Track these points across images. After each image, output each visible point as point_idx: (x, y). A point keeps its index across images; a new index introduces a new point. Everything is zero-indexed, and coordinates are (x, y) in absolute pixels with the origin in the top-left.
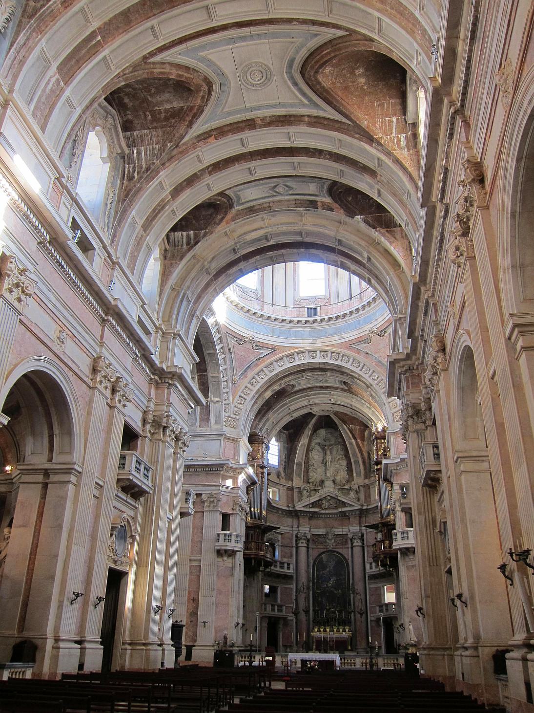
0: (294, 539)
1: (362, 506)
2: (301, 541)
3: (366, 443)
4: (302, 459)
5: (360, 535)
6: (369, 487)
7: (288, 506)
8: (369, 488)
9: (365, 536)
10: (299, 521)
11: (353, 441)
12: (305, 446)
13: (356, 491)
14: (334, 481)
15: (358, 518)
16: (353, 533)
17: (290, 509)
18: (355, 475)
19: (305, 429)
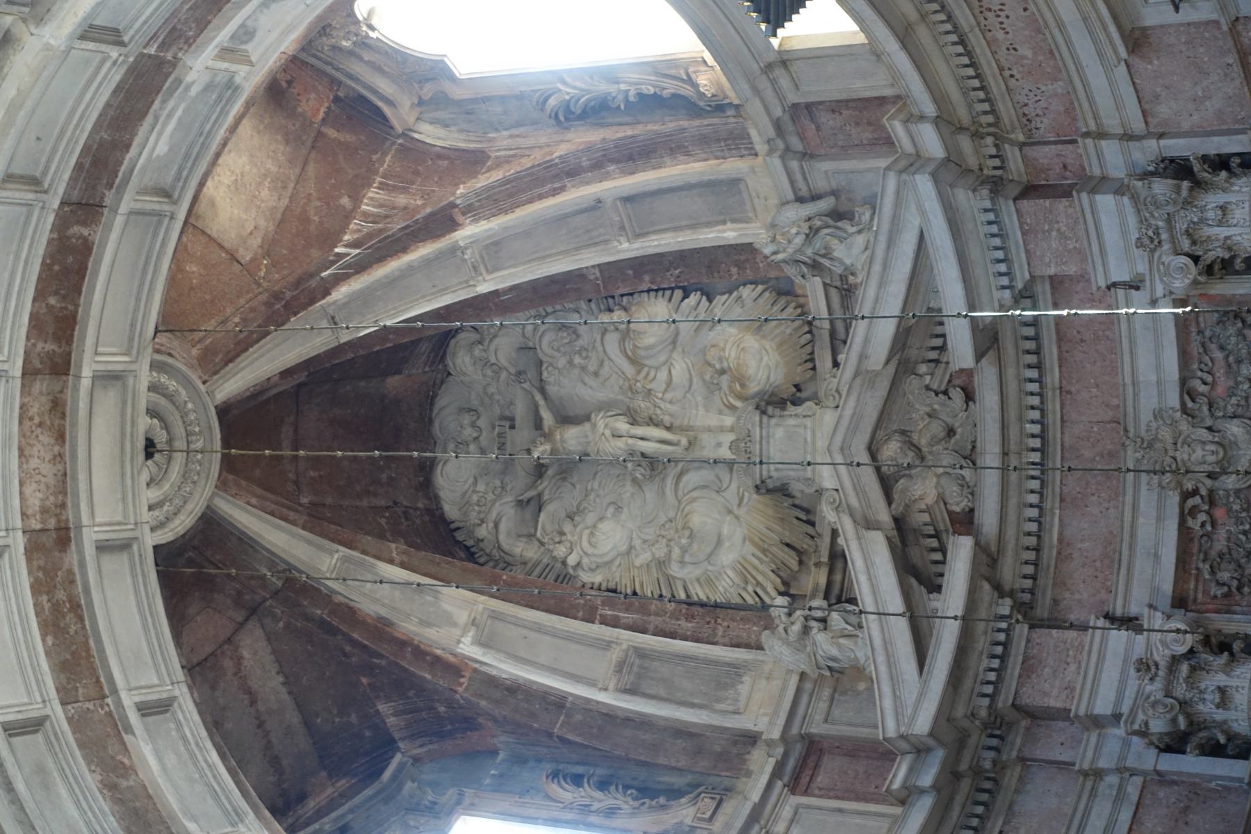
0: (1191, 764)
1: (915, 162)
2: (1207, 709)
3: (501, 142)
4: (608, 645)
5: (1161, 187)
6: (795, 106)
7: (905, 798)
8: (808, 106)
9: (1176, 147)
10: (1063, 715)
11: (469, 231)
12: (495, 616)
13: (838, 215)
14: (774, 402)
15: (1025, 204)
16: (1149, 243)
17: (927, 779)
18: (729, 234)
19: (349, 613)
